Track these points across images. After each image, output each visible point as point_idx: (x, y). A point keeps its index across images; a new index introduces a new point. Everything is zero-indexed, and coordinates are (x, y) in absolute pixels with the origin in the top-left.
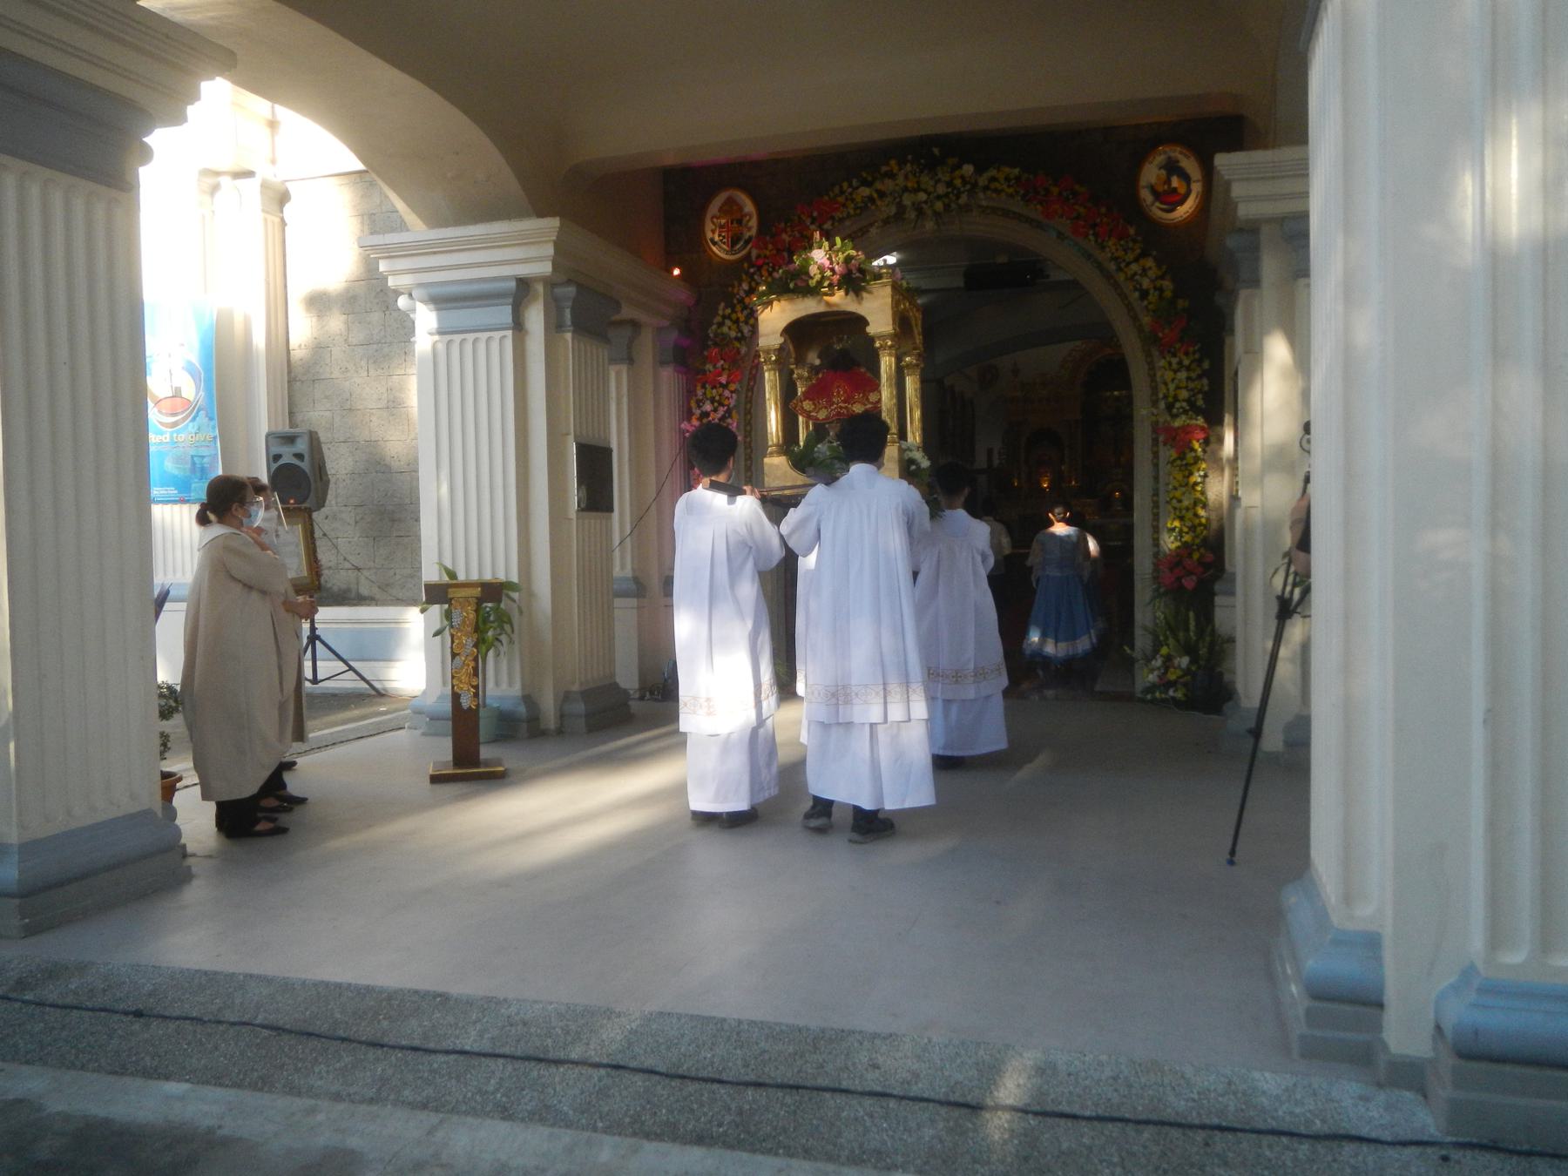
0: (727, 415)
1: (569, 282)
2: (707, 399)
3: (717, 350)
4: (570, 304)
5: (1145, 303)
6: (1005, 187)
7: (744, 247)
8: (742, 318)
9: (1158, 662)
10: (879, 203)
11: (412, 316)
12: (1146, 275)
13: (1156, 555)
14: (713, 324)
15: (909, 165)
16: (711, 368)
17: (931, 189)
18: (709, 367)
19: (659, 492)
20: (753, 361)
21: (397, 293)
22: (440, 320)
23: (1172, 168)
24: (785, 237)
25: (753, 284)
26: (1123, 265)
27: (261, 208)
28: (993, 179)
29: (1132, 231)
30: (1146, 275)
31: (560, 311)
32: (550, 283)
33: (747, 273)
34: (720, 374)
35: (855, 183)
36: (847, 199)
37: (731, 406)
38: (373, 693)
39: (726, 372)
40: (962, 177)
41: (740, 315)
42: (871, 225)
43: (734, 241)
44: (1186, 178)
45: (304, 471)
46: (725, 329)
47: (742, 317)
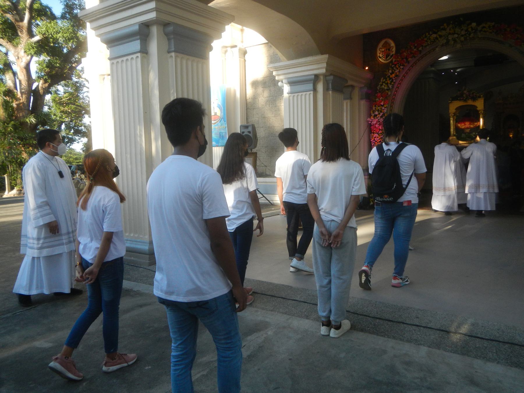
1: (331, 75)
2: (376, 110)
3: (380, 94)
4: (331, 82)
7: (390, 58)
8: (389, 83)
10: (439, 39)
11: (283, 88)
14: (379, 85)
15: (451, 25)
17: (459, 33)
18: (377, 99)
20: (393, 97)
21: (278, 81)
22: (291, 89)
24: (405, 54)
25: (393, 71)
27: (238, 56)
28: (484, 27)
31: (328, 84)
32: (325, 76)
33: (391, 67)
35: (431, 33)
36: (428, 39)
37: (385, 112)
38: (270, 204)
40: (472, 27)
41: (388, 81)
42: (437, 47)
43: (387, 57)
45: (250, 136)
46: (383, 87)
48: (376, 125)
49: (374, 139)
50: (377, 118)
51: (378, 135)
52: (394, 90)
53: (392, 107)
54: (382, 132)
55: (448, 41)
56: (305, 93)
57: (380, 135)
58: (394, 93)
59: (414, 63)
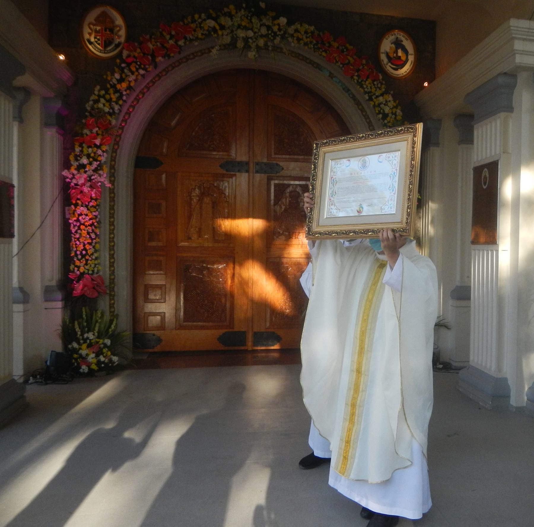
0: (99, 168)
3: (93, 119)
5: (386, 121)
7: (113, 50)
8: (114, 100)
10: (220, 33)
12: (387, 105)
14: (90, 101)
17: (256, 30)
18: (86, 131)
19: (42, 222)
23: (398, 44)
25: (124, 76)
26: (373, 97)
29: (381, 77)
30: (387, 105)
34: (96, 139)
35: (203, 16)
36: (197, 27)
37: (102, 162)
41: (112, 96)
42: (213, 48)
44: (406, 52)
46: (100, 105)
47: (114, 97)
48: (81, 186)
50: (85, 172)
51: (88, 209)
52: (121, 117)
53: (116, 152)
54: (97, 205)
57: (93, 209)
58: (121, 125)
59: (164, 70)
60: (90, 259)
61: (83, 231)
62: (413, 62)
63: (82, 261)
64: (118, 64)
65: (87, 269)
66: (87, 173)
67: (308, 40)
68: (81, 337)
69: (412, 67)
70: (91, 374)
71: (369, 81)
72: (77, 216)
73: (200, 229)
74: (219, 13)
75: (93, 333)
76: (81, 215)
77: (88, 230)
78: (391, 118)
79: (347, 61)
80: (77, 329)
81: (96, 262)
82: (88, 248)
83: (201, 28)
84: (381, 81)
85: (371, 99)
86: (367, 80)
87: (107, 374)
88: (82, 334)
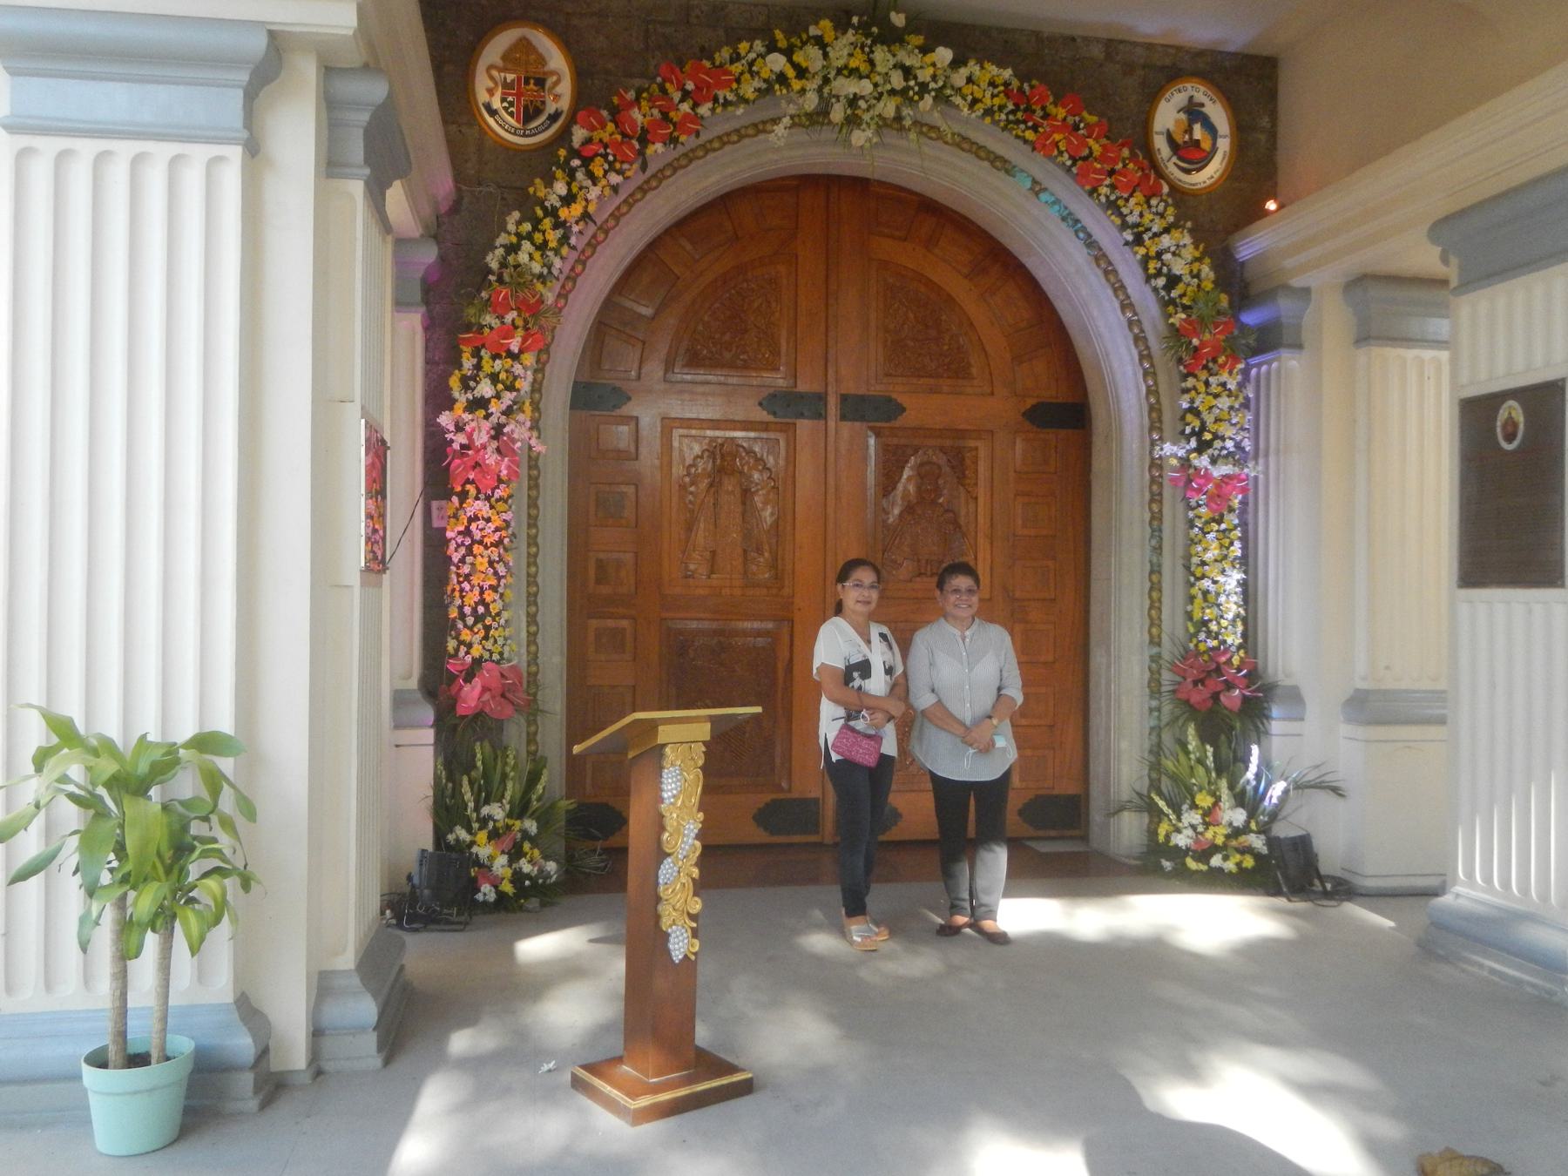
0: (515, 407)
1: (368, 68)
4: (365, 117)
5: (1174, 294)
6: (988, 94)
9: (1193, 817)
10: (797, 85)
12: (1179, 256)
13: (1155, 659)
14: (496, 248)
16: (493, 325)
18: (489, 319)
23: (1193, 112)
24: (636, 115)
25: (575, 190)
26: (1145, 237)
34: (513, 337)
35: (759, 46)
37: (522, 392)
39: (520, 333)
40: (934, 65)
42: (775, 121)
43: (530, 113)
46: (523, 257)
47: (553, 237)
48: (478, 451)
49: (467, 528)
50: (487, 417)
51: (492, 507)
54: (510, 496)
55: (823, 112)
56: (173, 148)
57: (501, 506)
60: (495, 625)
61: (479, 558)
62: (1228, 154)
63: (476, 630)
64: (562, 159)
65: (489, 650)
66: (491, 419)
67: (997, 101)
68: (475, 815)
69: (1227, 166)
70: (503, 903)
71: (1139, 197)
72: (466, 523)
73: (714, 553)
74: (793, 40)
75: (499, 804)
76: (475, 518)
77: (489, 557)
78: (1188, 285)
79: (1086, 152)
80: (468, 796)
81: (507, 633)
82: (488, 599)
83: (753, 74)
84: (1164, 198)
85: (1138, 240)
86: (1131, 195)
87: (543, 905)
88: (477, 809)
